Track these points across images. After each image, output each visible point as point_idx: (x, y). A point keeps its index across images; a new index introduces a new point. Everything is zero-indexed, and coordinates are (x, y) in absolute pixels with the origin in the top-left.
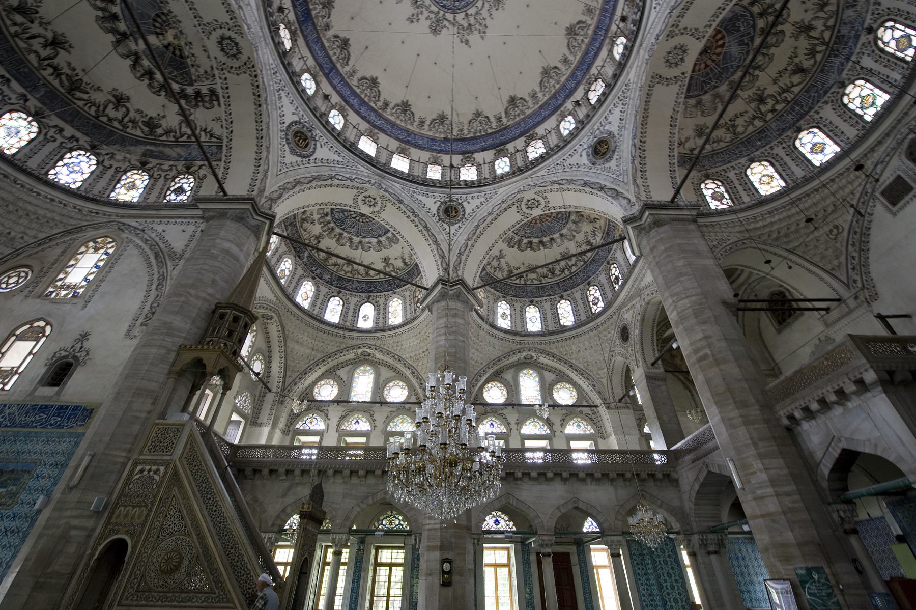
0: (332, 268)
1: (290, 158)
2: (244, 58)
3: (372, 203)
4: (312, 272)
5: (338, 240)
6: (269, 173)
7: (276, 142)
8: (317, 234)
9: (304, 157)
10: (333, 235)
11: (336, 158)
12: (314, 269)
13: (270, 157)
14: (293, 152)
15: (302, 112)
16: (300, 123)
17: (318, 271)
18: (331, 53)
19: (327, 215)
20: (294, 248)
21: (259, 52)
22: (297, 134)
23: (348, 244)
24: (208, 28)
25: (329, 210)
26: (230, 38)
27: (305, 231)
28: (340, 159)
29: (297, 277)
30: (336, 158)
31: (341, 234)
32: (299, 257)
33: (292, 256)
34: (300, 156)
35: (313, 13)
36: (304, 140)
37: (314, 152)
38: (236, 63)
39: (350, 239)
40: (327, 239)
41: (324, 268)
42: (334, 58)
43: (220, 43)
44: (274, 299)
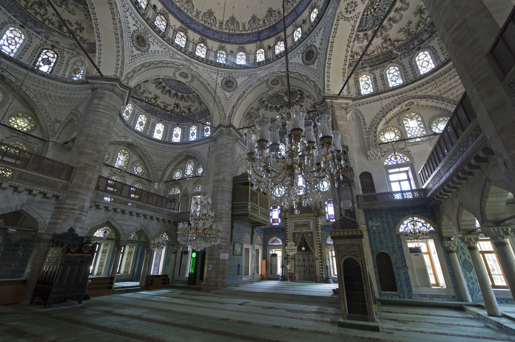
0: (419, 29)
1: (314, 67)
2: (277, 79)
3: (353, 5)
4: (413, 49)
5: (395, 22)
6: (317, 83)
7: (307, 72)
8: (382, 40)
9: (317, 56)
10: (388, 27)
11: (322, 31)
12: (412, 47)
13: (312, 79)
14: (313, 63)
15: (299, 51)
16: (303, 53)
17: (416, 43)
18: (289, 11)
19: (366, 35)
20: (384, 62)
21: (275, 71)
22: (307, 58)
23: (402, 12)
24: (270, 89)
25: (361, 34)
26: (272, 82)
27: (374, 52)
28: (323, 28)
29: (407, 66)
30: (322, 31)
31: (390, 19)
32: (394, 58)
33: (390, 65)
34: (316, 59)
35: (274, 23)
36: (310, 53)
37: (316, 49)
38: (280, 81)
39: (396, 10)
40: (389, 33)
41: (416, 36)
42: (292, 9)
43: (275, 85)
44: (396, 97)
